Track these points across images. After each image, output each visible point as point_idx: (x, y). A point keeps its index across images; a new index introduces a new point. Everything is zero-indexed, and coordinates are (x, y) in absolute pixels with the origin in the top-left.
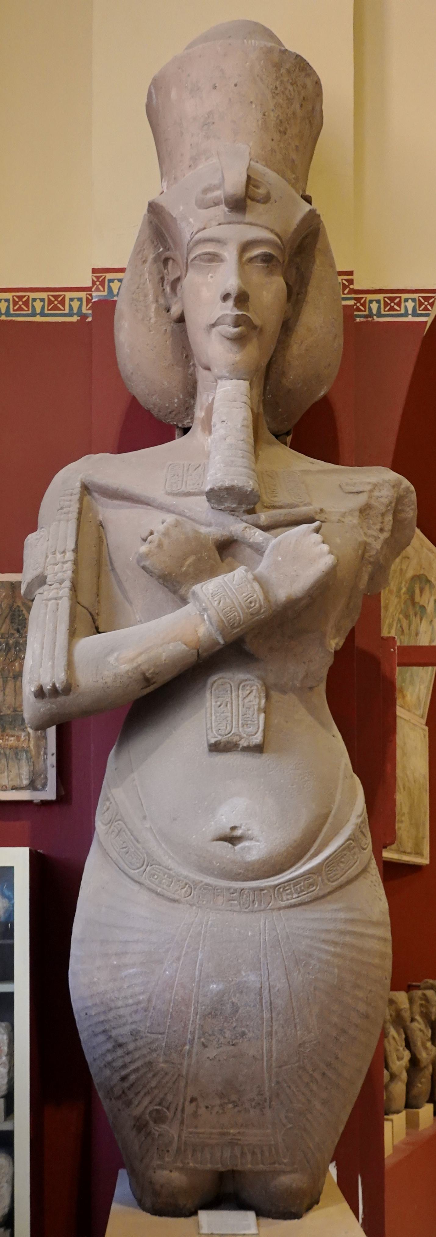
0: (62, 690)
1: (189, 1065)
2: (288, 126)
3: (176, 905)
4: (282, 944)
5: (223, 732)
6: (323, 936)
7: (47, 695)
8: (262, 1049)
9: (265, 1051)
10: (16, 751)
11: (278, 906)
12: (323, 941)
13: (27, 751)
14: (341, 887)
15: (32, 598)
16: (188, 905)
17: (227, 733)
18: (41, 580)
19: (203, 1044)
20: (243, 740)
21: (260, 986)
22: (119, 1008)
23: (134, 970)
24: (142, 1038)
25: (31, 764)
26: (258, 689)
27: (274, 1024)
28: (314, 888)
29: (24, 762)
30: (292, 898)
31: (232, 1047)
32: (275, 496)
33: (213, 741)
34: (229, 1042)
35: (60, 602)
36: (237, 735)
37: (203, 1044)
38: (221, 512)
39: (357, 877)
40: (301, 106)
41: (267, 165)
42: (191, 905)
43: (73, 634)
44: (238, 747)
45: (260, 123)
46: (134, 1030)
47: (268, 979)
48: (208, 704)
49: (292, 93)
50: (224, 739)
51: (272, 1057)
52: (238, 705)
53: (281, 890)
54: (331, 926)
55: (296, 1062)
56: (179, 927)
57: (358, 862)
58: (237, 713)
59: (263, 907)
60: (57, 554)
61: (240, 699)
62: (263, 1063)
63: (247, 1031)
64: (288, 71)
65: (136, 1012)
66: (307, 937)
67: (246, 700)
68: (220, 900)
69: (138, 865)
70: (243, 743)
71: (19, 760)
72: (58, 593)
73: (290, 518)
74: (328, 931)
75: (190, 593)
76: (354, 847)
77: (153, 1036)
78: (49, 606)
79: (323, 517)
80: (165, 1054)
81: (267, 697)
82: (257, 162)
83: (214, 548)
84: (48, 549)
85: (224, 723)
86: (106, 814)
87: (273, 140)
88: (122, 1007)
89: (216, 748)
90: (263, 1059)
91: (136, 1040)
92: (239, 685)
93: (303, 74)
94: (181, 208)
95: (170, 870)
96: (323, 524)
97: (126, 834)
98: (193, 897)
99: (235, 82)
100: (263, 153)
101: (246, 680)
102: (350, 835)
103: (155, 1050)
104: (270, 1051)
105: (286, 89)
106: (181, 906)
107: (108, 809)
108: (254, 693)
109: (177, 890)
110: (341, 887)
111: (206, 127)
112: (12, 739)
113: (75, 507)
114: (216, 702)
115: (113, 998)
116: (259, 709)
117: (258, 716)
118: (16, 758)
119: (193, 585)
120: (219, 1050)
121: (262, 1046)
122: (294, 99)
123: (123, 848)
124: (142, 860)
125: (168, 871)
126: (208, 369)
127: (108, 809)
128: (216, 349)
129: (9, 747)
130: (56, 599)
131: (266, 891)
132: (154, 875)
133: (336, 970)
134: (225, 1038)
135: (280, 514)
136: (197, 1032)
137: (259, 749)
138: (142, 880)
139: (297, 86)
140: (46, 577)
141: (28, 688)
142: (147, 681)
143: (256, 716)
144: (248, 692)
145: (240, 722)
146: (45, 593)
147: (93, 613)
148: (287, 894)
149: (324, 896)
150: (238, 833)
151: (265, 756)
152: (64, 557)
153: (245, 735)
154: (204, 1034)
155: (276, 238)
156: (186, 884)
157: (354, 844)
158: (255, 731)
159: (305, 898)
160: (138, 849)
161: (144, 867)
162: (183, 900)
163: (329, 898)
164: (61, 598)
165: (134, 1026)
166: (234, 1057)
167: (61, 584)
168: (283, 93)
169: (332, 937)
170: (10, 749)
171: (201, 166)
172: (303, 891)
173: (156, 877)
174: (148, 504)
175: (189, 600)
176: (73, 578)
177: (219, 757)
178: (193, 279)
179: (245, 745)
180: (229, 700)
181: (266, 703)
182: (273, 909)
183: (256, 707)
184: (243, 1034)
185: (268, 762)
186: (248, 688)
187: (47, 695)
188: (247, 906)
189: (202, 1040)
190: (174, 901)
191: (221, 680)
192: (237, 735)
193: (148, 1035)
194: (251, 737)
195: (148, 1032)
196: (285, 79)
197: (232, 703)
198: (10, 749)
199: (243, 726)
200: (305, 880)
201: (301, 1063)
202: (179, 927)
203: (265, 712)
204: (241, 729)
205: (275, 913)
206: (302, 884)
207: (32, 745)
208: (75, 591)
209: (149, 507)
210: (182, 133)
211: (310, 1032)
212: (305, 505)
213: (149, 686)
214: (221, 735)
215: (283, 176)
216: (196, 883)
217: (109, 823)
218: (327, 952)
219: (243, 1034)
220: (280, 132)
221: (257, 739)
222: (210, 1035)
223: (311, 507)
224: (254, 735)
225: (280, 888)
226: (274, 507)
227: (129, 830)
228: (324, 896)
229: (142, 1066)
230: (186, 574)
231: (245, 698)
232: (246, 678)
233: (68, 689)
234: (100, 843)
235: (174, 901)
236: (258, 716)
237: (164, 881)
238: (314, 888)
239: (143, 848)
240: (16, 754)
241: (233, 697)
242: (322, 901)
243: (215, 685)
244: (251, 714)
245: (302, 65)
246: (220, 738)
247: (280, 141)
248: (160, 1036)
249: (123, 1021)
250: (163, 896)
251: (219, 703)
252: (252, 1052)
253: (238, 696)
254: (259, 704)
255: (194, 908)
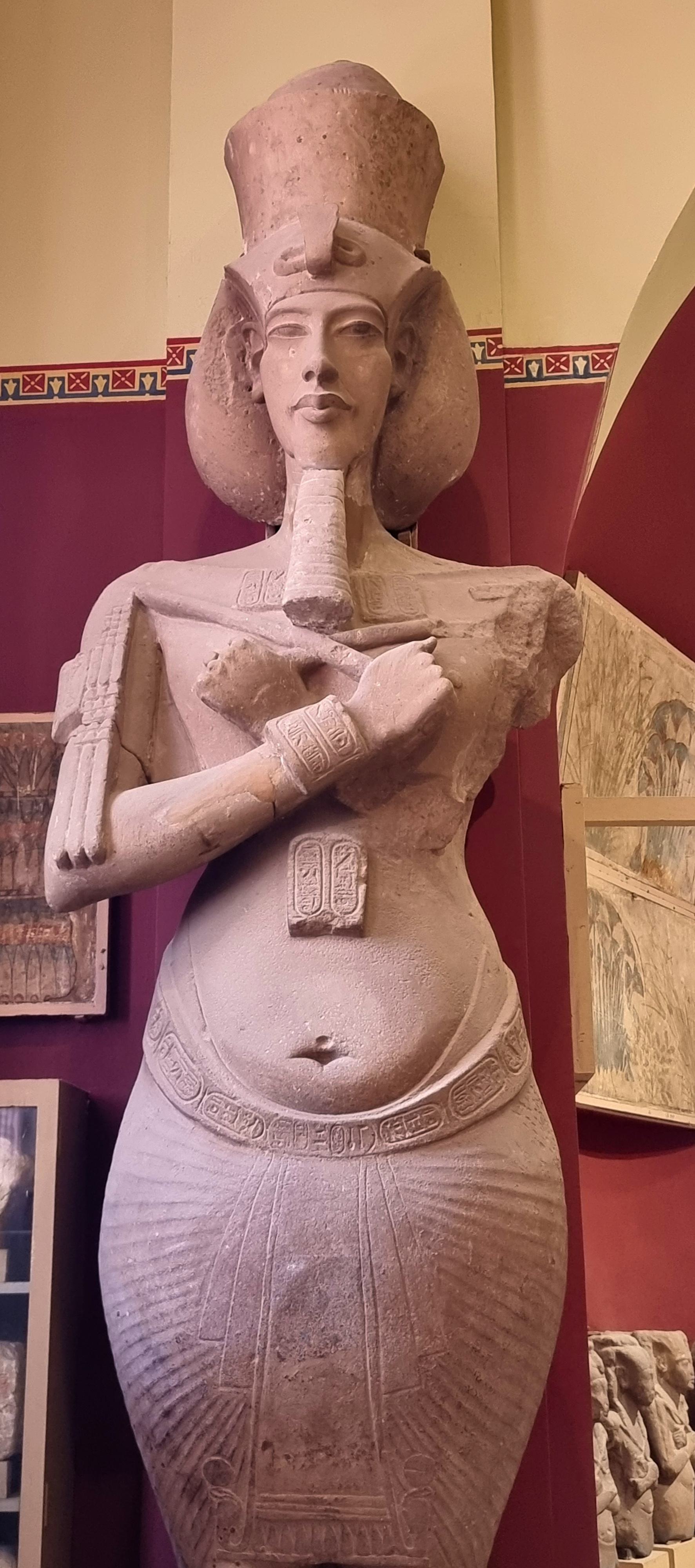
0: (93, 857)
1: (260, 1389)
2: (392, 177)
3: (242, 1149)
4: (389, 1205)
5: (308, 910)
6: (450, 1193)
7: (75, 864)
8: (365, 1364)
9: (368, 1366)
10: (53, 948)
11: (384, 1149)
12: (450, 1200)
13: (69, 947)
14: (476, 1123)
15: (65, 742)
16: (258, 1149)
17: (314, 910)
18: (76, 719)
19: (279, 1356)
20: (336, 920)
21: (358, 1266)
22: (161, 1302)
23: (182, 1244)
24: (191, 1346)
25: (73, 964)
26: (357, 851)
27: (381, 1324)
28: (436, 1124)
29: (63, 963)
30: (405, 1138)
31: (319, 1361)
32: (378, 608)
33: (295, 921)
34: (315, 1352)
35: (97, 745)
36: (328, 913)
37: (279, 1356)
38: (306, 630)
39: (502, 1109)
40: (409, 153)
41: (366, 222)
42: (263, 1149)
43: (112, 786)
44: (330, 930)
45: (355, 175)
46: (181, 1335)
47: (370, 1255)
48: (290, 873)
49: (396, 141)
50: (310, 918)
51: (379, 1376)
52: (330, 873)
53: (389, 1126)
54: (462, 1180)
55: (416, 1385)
56: (244, 1180)
57: (503, 1089)
58: (328, 884)
59: (362, 1151)
60: (99, 685)
61: (333, 866)
62: (366, 1386)
63: (341, 1336)
64: (390, 119)
65: (184, 1307)
66: (427, 1195)
67: (341, 867)
68: (303, 1141)
69: (193, 1094)
70: (337, 924)
71: (57, 960)
72: (95, 735)
73: (397, 633)
74: (456, 1186)
75: (264, 730)
76: (497, 1068)
77: (206, 1343)
78: (83, 751)
79: (440, 631)
80: (225, 1372)
81: (370, 862)
82: (353, 219)
83: (296, 674)
84: (88, 683)
85: (311, 898)
86: (156, 1025)
87: (372, 193)
88: (165, 1300)
89: (299, 931)
90: (366, 1379)
91: (184, 1350)
92: (332, 847)
93: (409, 119)
94: (258, 275)
95: (234, 1099)
96: (439, 641)
97: (178, 1051)
98: (265, 1138)
99: (325, 133)
100: (360, 208)
101: (341, 841)
102: (490, 1050)
103: (211, 1366)
104: (376, 1366)
105: (387, 137)
106: (248, 1150)
107: (158, 1018)
108: (351, 857)
109: (243, 1128)
110: (476, 1123)
111: (290, 183)
112: (48, 930)
113: (123, 628)
114: (301, 870)
115: (153, 1287)
116: (358, 879)
117: (357, 888)
118: (53, 958)
119: (268, 720)
120: (302, 1364)
121: (365, 1360)
122: (397, 149)
123: (173, 1071)
124: (197, 1086)
125: (231, 1101)
126: (293, 456)
127: (158, 1018)
128: (301, 438)
129: (43, 941)
130: (92, 742)
131: (366, 1128)
132: (213, 1107)
133: (470, 1245)
134: (310, 1346)
135: (383, 630)
136: (269, 1336)
137: (357, 932)
138: (196, 1114)
139: (402, 133)
140: (82, 715)
141: (51, 857)
142: (207, 843)
143: (353, 887)
144: (344, 856)
145: (332, 896)
146: (79, 735)
147: (142, 759)
148: (397, 1133)
149: (451, 1136)
150: (328, 1046)
151: (367, 940)
152: (106, 690)
153: (338, 913)
154: (280, 1338)
155: (377, 308)
156: (255, 1119)
157: (496, 1063)
158: (352, 908)
159: (424, 1137)
160: (193, 1071)
161: (200, 1096)
162: (251, 1141)
163: (457, 1139)
164: (99, 740)
165: (180, 1330)
166: (324, 1375)
167: (99, 723)
168: (384, 141)
169: (462, 1194)
170: (45, 945)
171: (283, 227)
172: (420, 1128)
173: (215, 1109)
174: (215, 622)
175: (263, 740)
176: (116, 716)
177: (305, 942)
178: (273, 354)
179: (339, 926)
180: (319, 866)
181: (367, 870)
182: (378, 1154)
183: (354, 876)
184: (336, 1340)
185: (372, 950)
186: (344, 850)
187: (75, 864)
188: (339, 1150)
189: (277, 1348)
190: (239, 1143)
191: (308, 842)
192: (328, 913)
193: (202, 1342)
194: (347, 916)
195: (200, 1338)
196: (387, 127)
197: (321, 872)
198: (45, 945)
199: (336, 902)
200: (423, 1111)
201: (423, 1387)
202: (244, 1180)
203: (366, 883)
204: (333, 905)
205: (380, 1160)
206: (419, 1117)
207: (75, 942)
208: (119, 731)
209: (217, 625)
210: (263, 191)
211: (433, 1339)
212: (418, 617)
213: (210, 851)
214: (306, 913)
215: (387, 233)
216: (270, 1117)
217: (157, 1038)
218: (456, 1216)
219: (336, 1340)
220: (381, 183)
221: (355, 917)
222: (288, 1342)
223: (425, 620)
224: (350, 913)
225: (386, 1124)
226: (376, 621)
227: (182, 1044)
228: (451, 1136)
229: (192, 1391)
230: (259, 706)
231: (339, 864)
232: (340, 838)
233: (103, 854)
234: (146, 1063)
235: (239, 1143)
236: (357, 888)
237: (226, 1115)
238: (436, 1124)
239: (199, 1069)
240: (53, 951)
241: (324, 863)
242: (449, 1142)
243: (300, 847)
244: (347, 885)
245: (407, 110)
246: (304, 917)
247: (382, 194)
248: (217, 1344)
249: (168, 1320)
250: (224, 1136)
251: (304, 872)
252: (350, 1368)
253: (331, 862)
254: (359, 871)
255: (267, 1152)
